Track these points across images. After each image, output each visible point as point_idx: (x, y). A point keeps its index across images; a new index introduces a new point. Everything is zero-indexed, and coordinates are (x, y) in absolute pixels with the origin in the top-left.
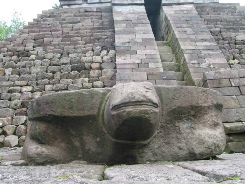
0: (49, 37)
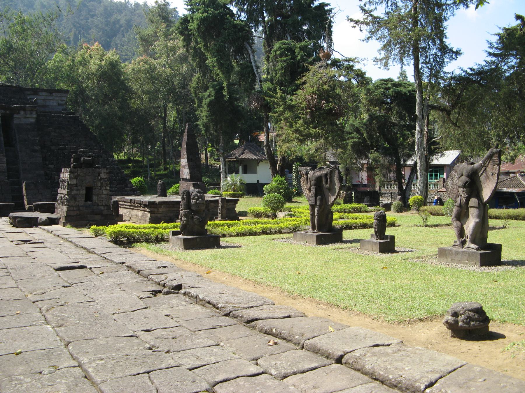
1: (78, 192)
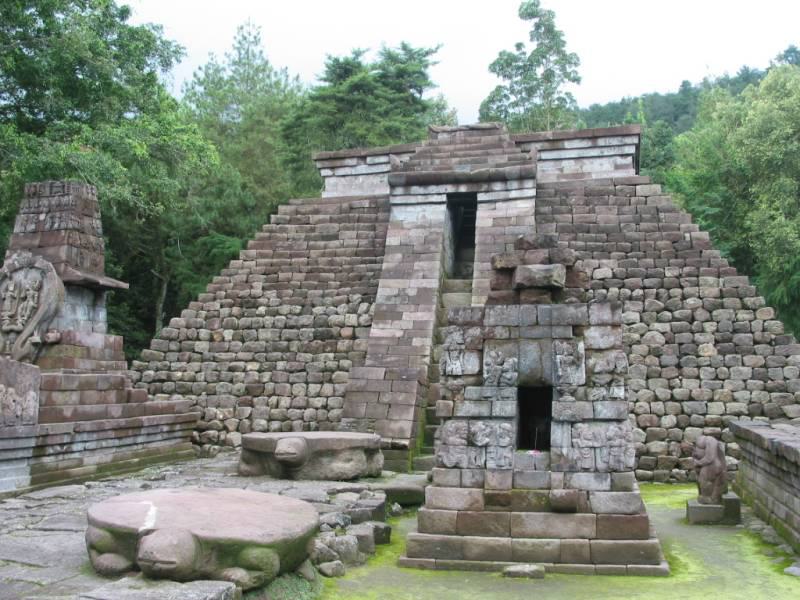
0: (287, 271)
1: (484, 410)
